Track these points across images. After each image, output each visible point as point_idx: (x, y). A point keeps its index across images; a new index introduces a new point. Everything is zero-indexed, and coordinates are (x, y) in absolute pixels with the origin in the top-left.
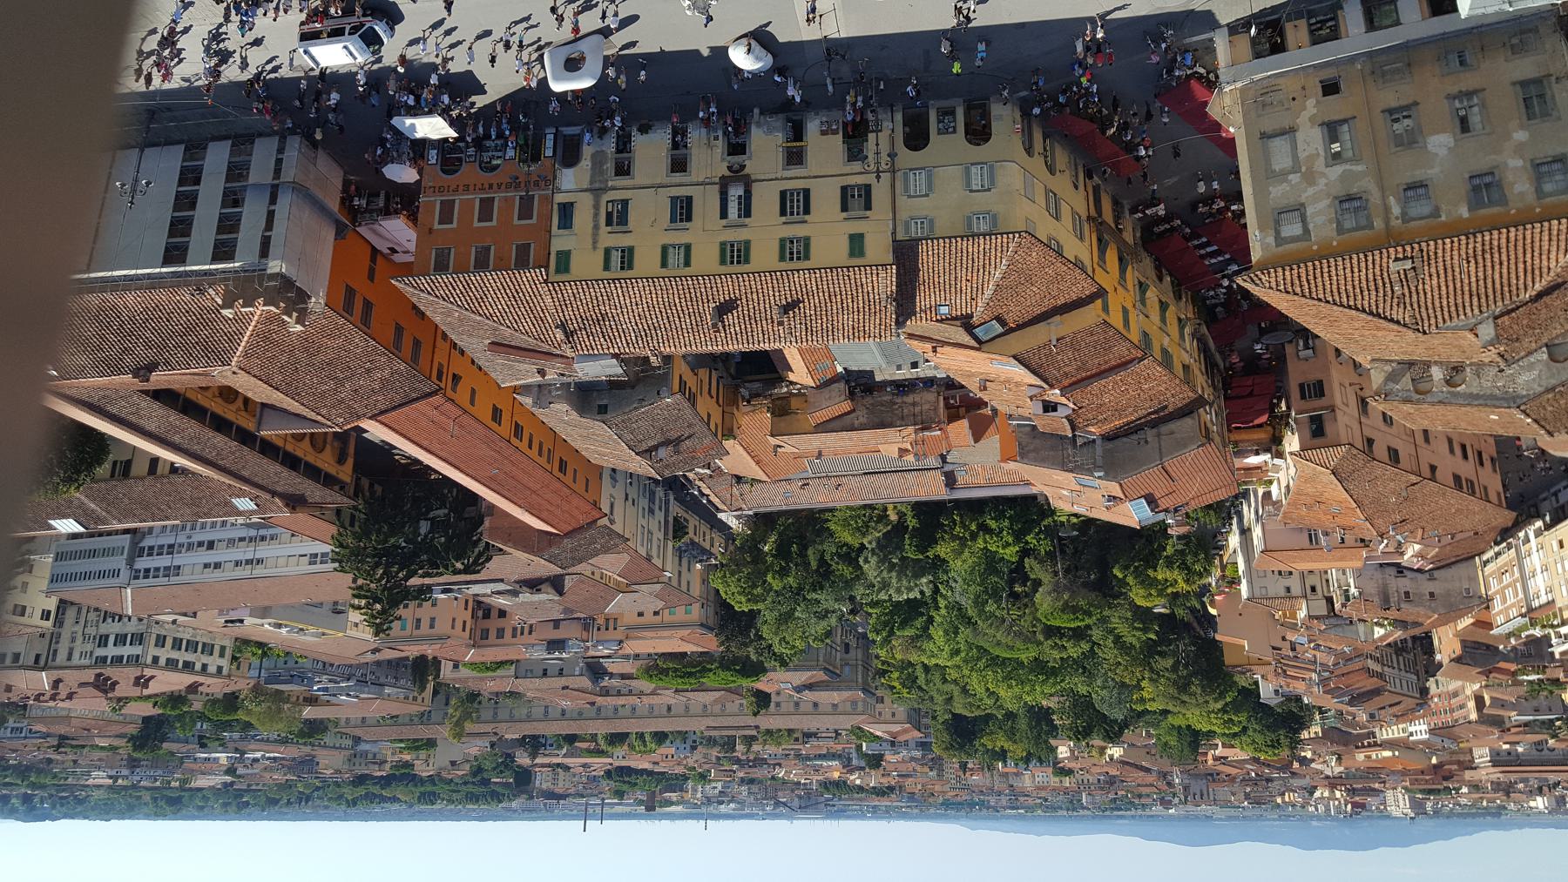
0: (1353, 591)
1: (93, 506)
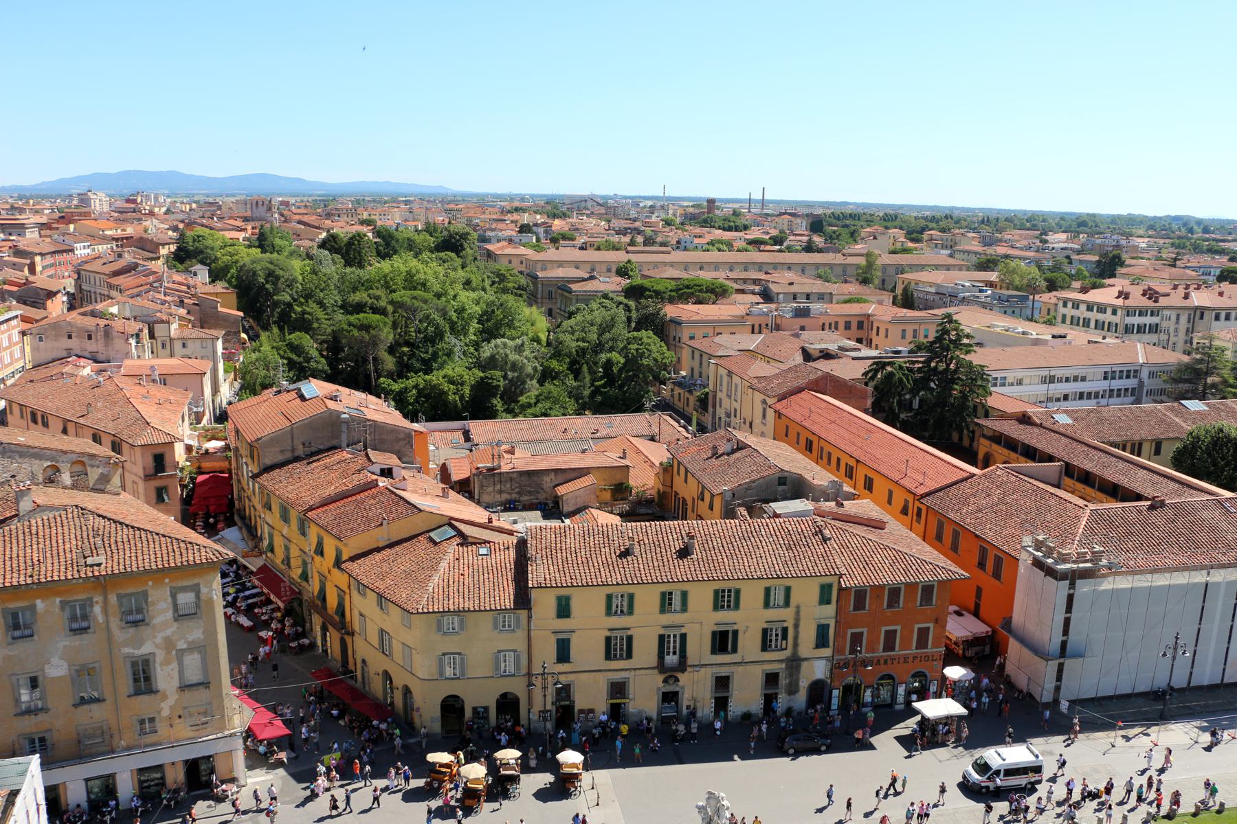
0: (133, 342)
1: (1177, 420)
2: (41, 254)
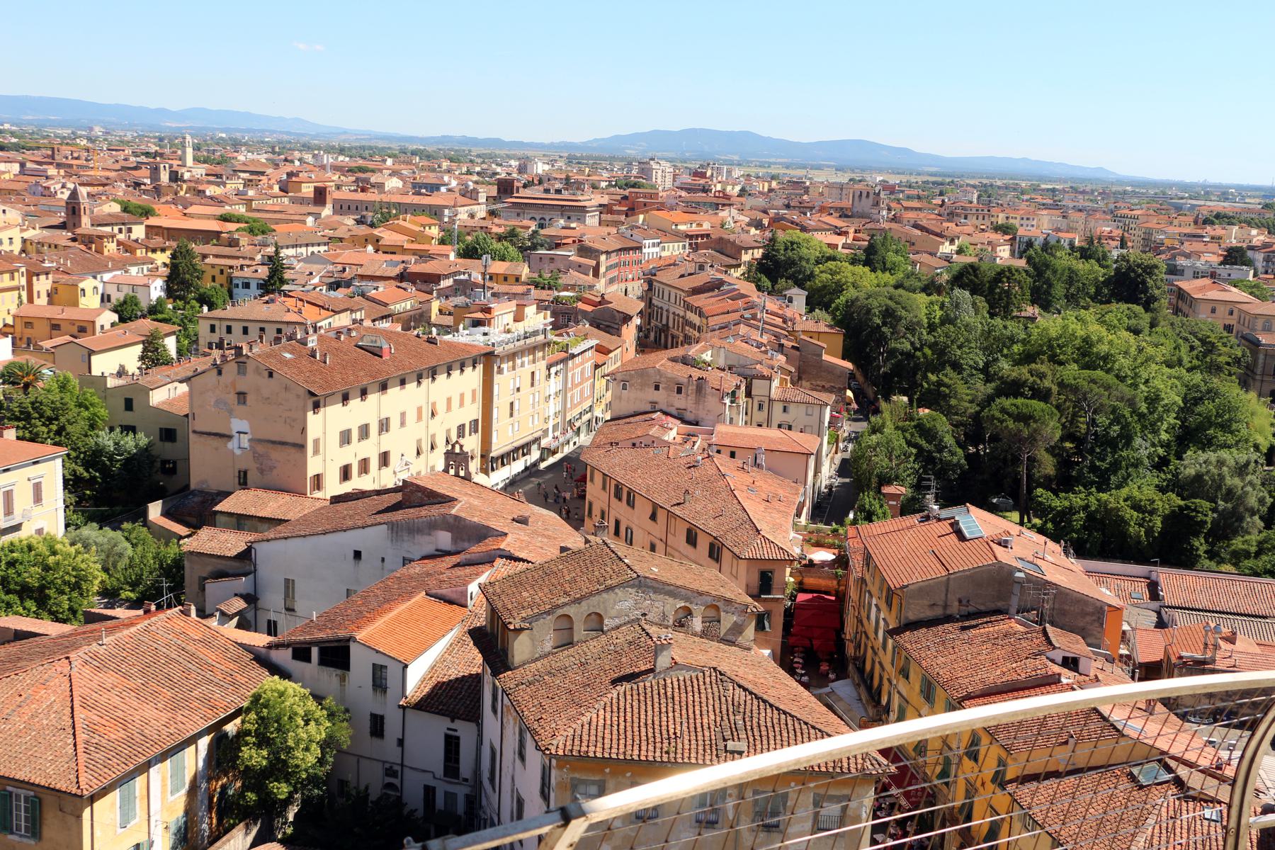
0: (727, 401)
2: (607, 253)
